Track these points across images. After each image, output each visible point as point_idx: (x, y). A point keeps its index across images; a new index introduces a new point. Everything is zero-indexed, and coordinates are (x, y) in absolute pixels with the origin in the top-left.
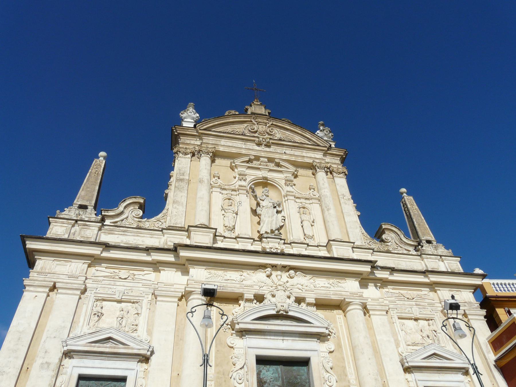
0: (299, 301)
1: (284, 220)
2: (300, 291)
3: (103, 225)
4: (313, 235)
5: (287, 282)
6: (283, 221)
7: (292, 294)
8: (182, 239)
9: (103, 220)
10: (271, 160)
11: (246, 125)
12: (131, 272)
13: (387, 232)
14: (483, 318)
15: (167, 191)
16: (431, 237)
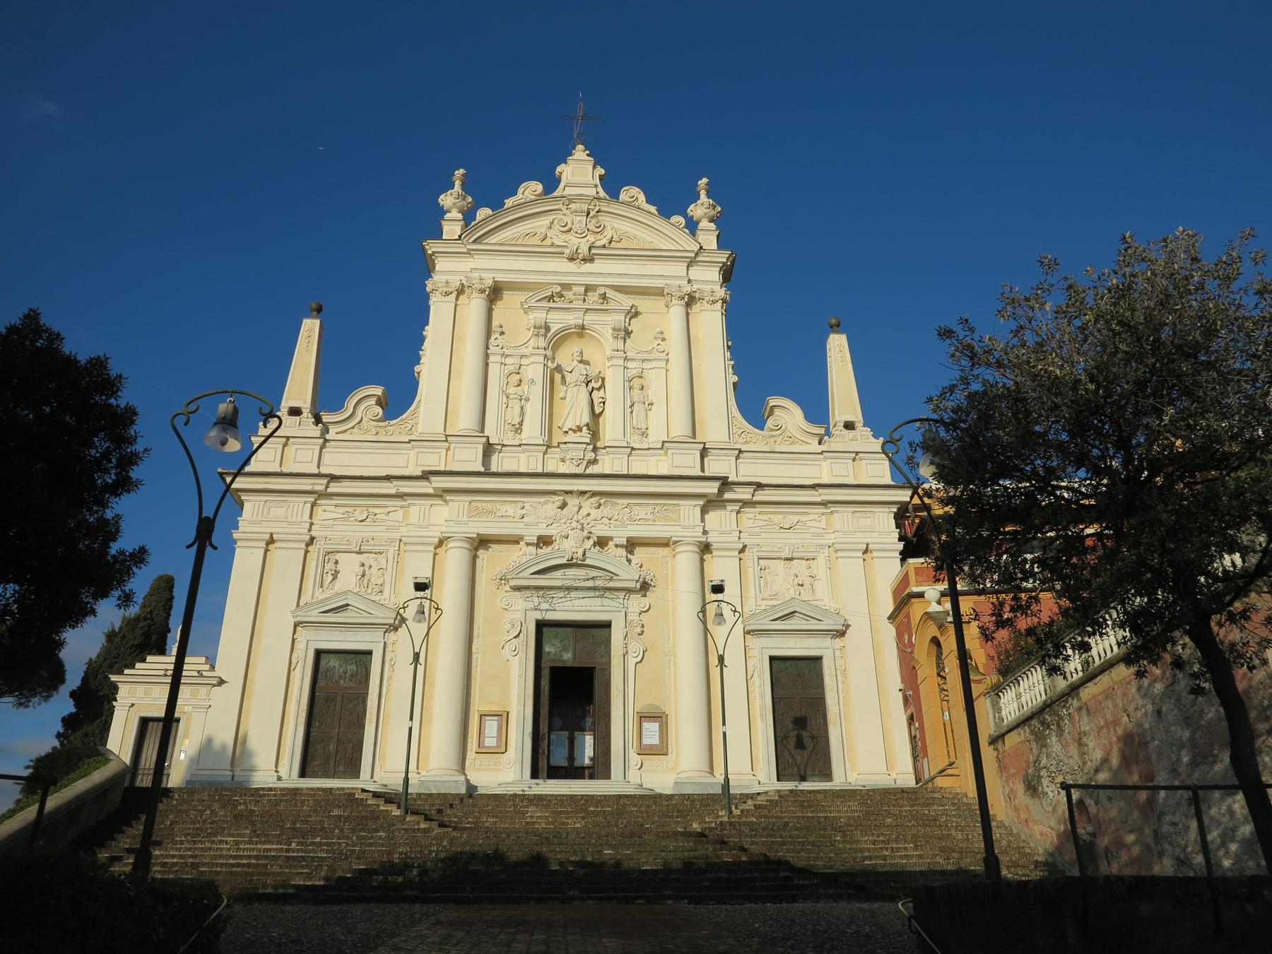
0: (602, 542)
1: (604, 403)
2: (607, 528)
3: (326, 441)
4: (647, 429)
5: (589, 515)
6: (602, 405)
7: (591, 533)
8: (434, 460)
9: (326, 431)
10: (589, 289)
11: (552, 218)
12: (371, 510)
13: (777, 412)
14: (898, 555)
15: (417, 368)
16: (856, 415)
